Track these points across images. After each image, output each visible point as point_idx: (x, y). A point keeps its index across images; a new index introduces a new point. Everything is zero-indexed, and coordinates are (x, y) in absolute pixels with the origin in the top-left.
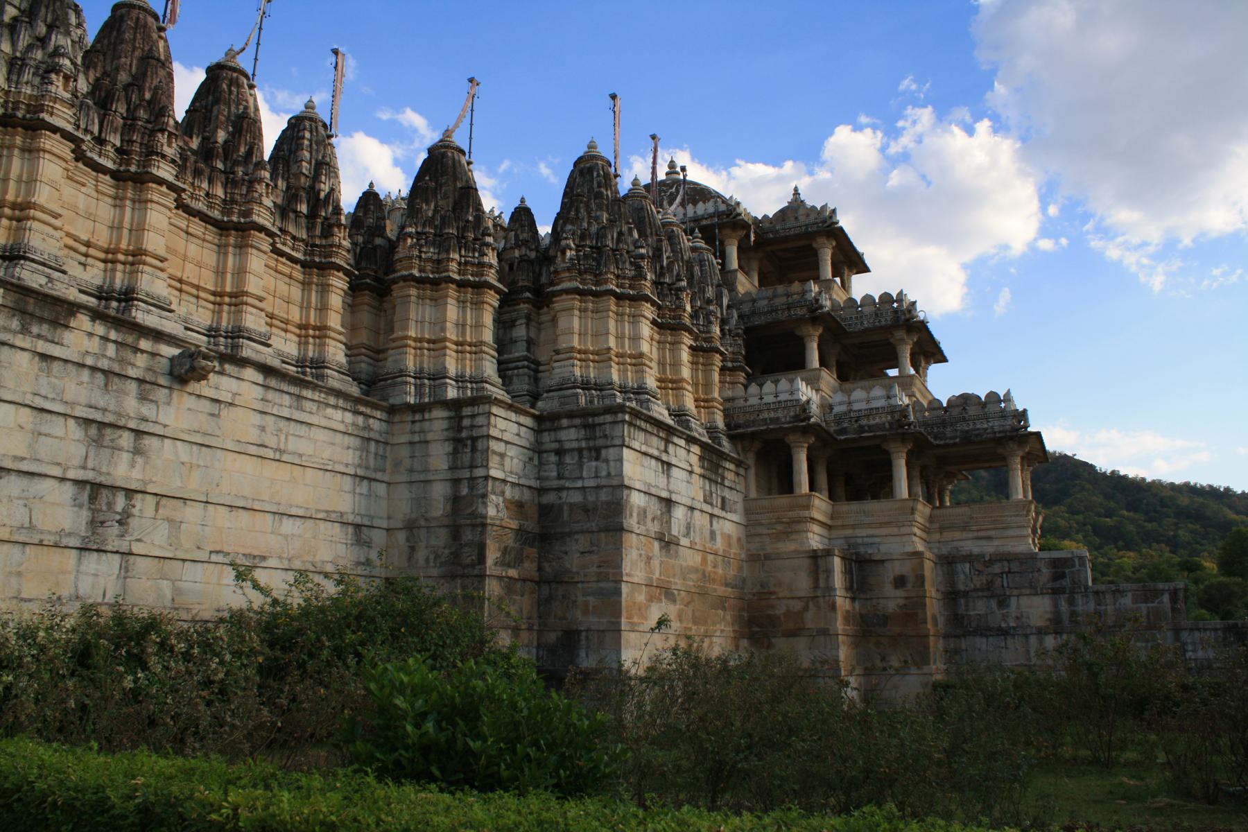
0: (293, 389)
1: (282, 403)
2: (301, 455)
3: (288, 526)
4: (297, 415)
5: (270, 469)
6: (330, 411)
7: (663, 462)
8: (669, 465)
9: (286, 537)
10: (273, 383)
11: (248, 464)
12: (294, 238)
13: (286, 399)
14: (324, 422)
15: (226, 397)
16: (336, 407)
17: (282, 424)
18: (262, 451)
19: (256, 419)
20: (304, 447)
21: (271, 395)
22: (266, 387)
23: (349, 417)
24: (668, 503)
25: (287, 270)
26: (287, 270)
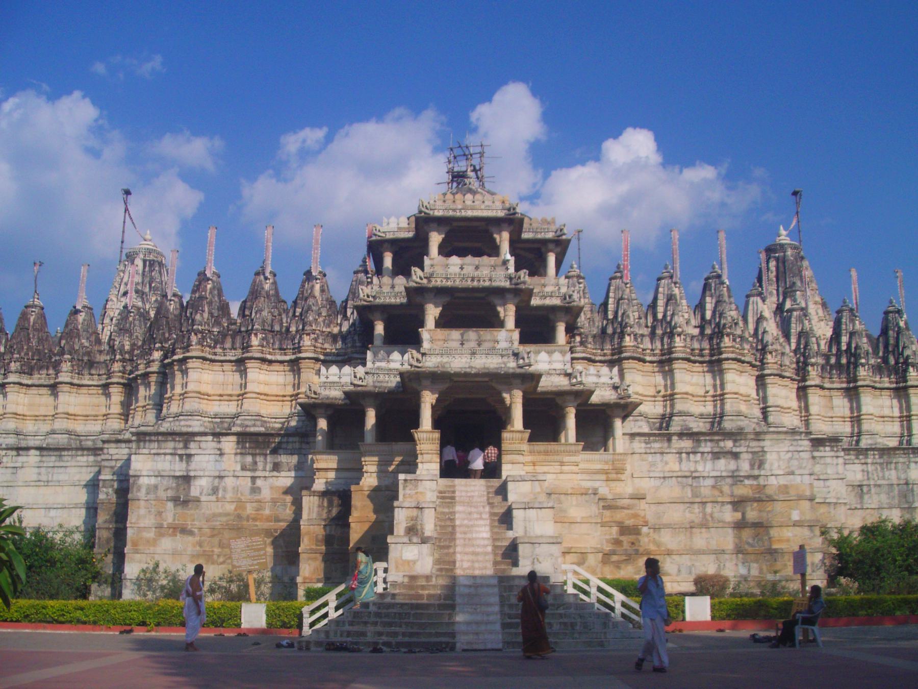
0: (56, 453)
1: (51, 460)
2: (59, 481)
3: (53, 513)
4: (62, 464)
5: (43, 490)
6: (79, 458)
7: (181, 456)
8: (189, 456)
9: (52, 518)
10: (45, 453)
11: (32, 490)
12: (99, 375)
13: (53, 458)
14: (73, 464)
15: (19, 465)
16: (83, 455)
17: (50, 470)
18: (38, 483)
19: (36, 470)
20: (62, 477)
21: (44, 459)
22: (42, 456)
23: (91, 458)
24: (187, 479)
25: (95, 392)
26: (95, 392)
